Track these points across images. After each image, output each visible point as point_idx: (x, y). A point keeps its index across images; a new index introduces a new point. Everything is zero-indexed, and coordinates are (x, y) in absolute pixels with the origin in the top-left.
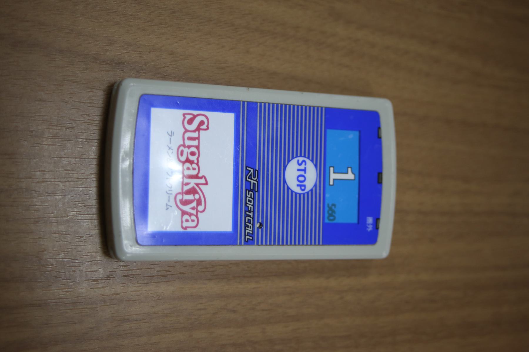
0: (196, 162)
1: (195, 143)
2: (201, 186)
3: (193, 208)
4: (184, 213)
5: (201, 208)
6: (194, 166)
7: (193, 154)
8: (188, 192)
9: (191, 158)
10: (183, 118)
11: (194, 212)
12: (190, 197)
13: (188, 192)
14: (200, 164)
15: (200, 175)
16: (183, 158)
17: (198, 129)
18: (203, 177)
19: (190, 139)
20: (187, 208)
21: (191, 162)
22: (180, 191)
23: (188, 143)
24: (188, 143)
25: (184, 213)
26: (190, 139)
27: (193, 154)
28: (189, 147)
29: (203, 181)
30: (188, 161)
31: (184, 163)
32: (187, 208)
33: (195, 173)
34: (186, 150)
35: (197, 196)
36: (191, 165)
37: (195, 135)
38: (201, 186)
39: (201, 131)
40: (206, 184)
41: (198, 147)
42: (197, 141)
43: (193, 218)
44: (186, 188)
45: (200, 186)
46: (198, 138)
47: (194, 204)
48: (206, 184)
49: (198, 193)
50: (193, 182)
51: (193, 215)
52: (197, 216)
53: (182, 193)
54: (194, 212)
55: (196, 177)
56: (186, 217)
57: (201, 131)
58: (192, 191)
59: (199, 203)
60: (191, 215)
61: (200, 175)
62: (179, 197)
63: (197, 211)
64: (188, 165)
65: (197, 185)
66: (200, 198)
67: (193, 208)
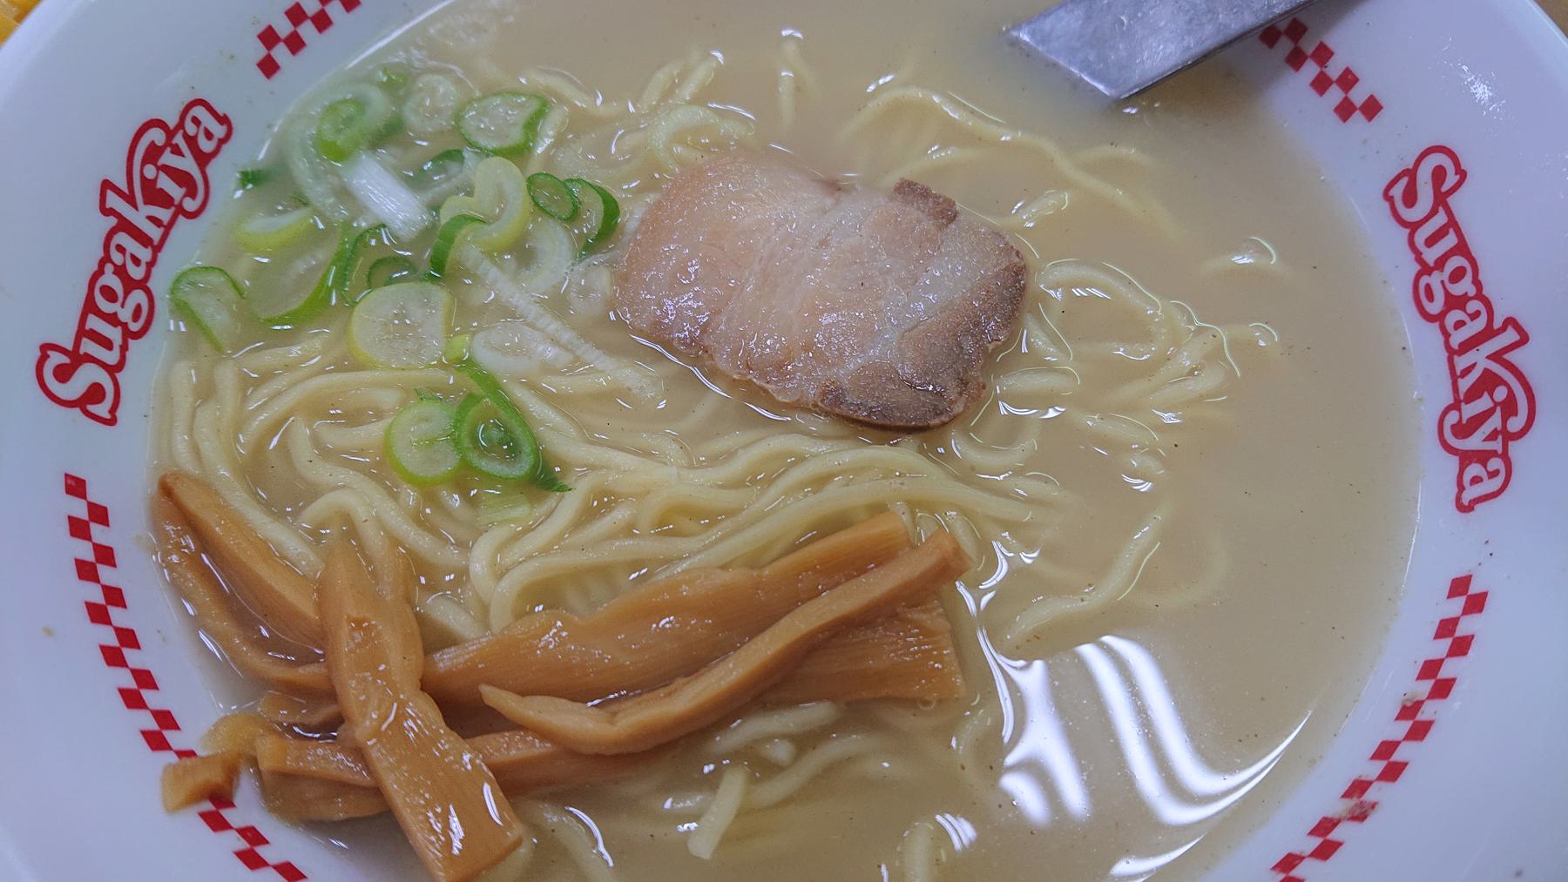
0: (109, 268)
1: (94, 323)
2: (125, 190)
3: (177, 151)
4: (203, 159)
5: (156, 135)
6: (117, 258)
7: (109, 294)
8: (164, 200)
9: (115, 283)
10: (119, 413)
11: (179, 140)
12: (166, 184)
13: (164, 200)
14: (100, 254)
15: (113, 221)
16: (138, 297)
18: (106, 211)
19: (107, 344)
20: (187, 164)
21: (120, 271)
22: (181, 219)
23: (115, 334)
24: (115, 334)
25: (203, 159)
26: (107, 344)
27: (109, 294)
28: (112, 319)
29: (113, 201)
30: (130, 285)
31: (142, 284)
32: (187, 164)
33: (122, 238)
34: (125, 315)
35: (150, 172)
36: (124, 265)
38: (124, 187)
39: (69, 346)
40: (107, 185)
41: (90, 307)
42: (88, 326)
43: (191, 128)
44: (164, 214)
45: (125, 190)
47: (168, 159)
48: (107, 185)
50: (139, 216)
51: (186, 137)
52: (181, 125)
53: (180, 211)
54: (179, 140)
55: (124, 225)
56: (206, 146)
57: (69, 346)
58: (155, 196)
59: (153, 154)
60: (191, 141)
61: (113, 221)
62: (190, 205)
63: (170, 134)
64: (136, 273)
65: (130, 199)
66: (144, 162)
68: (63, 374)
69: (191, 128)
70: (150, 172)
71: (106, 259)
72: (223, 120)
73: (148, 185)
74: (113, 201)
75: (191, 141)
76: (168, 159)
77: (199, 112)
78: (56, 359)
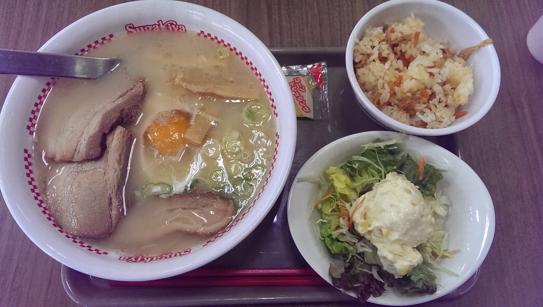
1: (142, 28)
3: (176, 27)
5: (175, 23)
6: (154, 26)
8: (168, 29)
11: (177, 26)
12: (170, 28)
17: (134, 28)
18: (158, 22)
20: (176, 29)
21: (153, 29)
27: (148, 28)
29: (160, 22)
32: (176, 29)
35: (169, 25)
37: (138, 29)
39: (135, 26)
41: (144, 27)
43: (180, 27)
46: (139, 27)
47: (174, 26)
49: (167, 25)
55: (159, 25)
59: (172, 24)
60: (179, 29)
65: (163, 25)
67: (176, 27)
68: (130, 27)
69: (180, 27)
70: (169, 25)
71: (152, 26)
72: (186, 31)
73: (167, 25)
74: (160, 22)
75: (179, 29)
76: (174, 26)
77: (183, 27)
78: (131, 26)
